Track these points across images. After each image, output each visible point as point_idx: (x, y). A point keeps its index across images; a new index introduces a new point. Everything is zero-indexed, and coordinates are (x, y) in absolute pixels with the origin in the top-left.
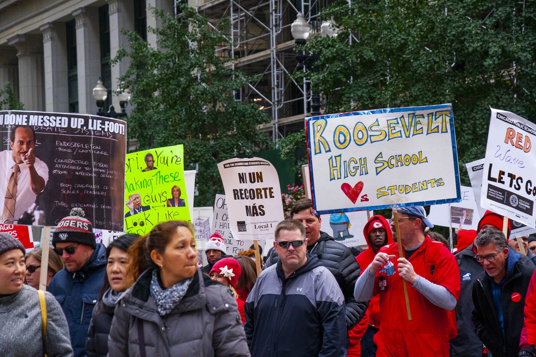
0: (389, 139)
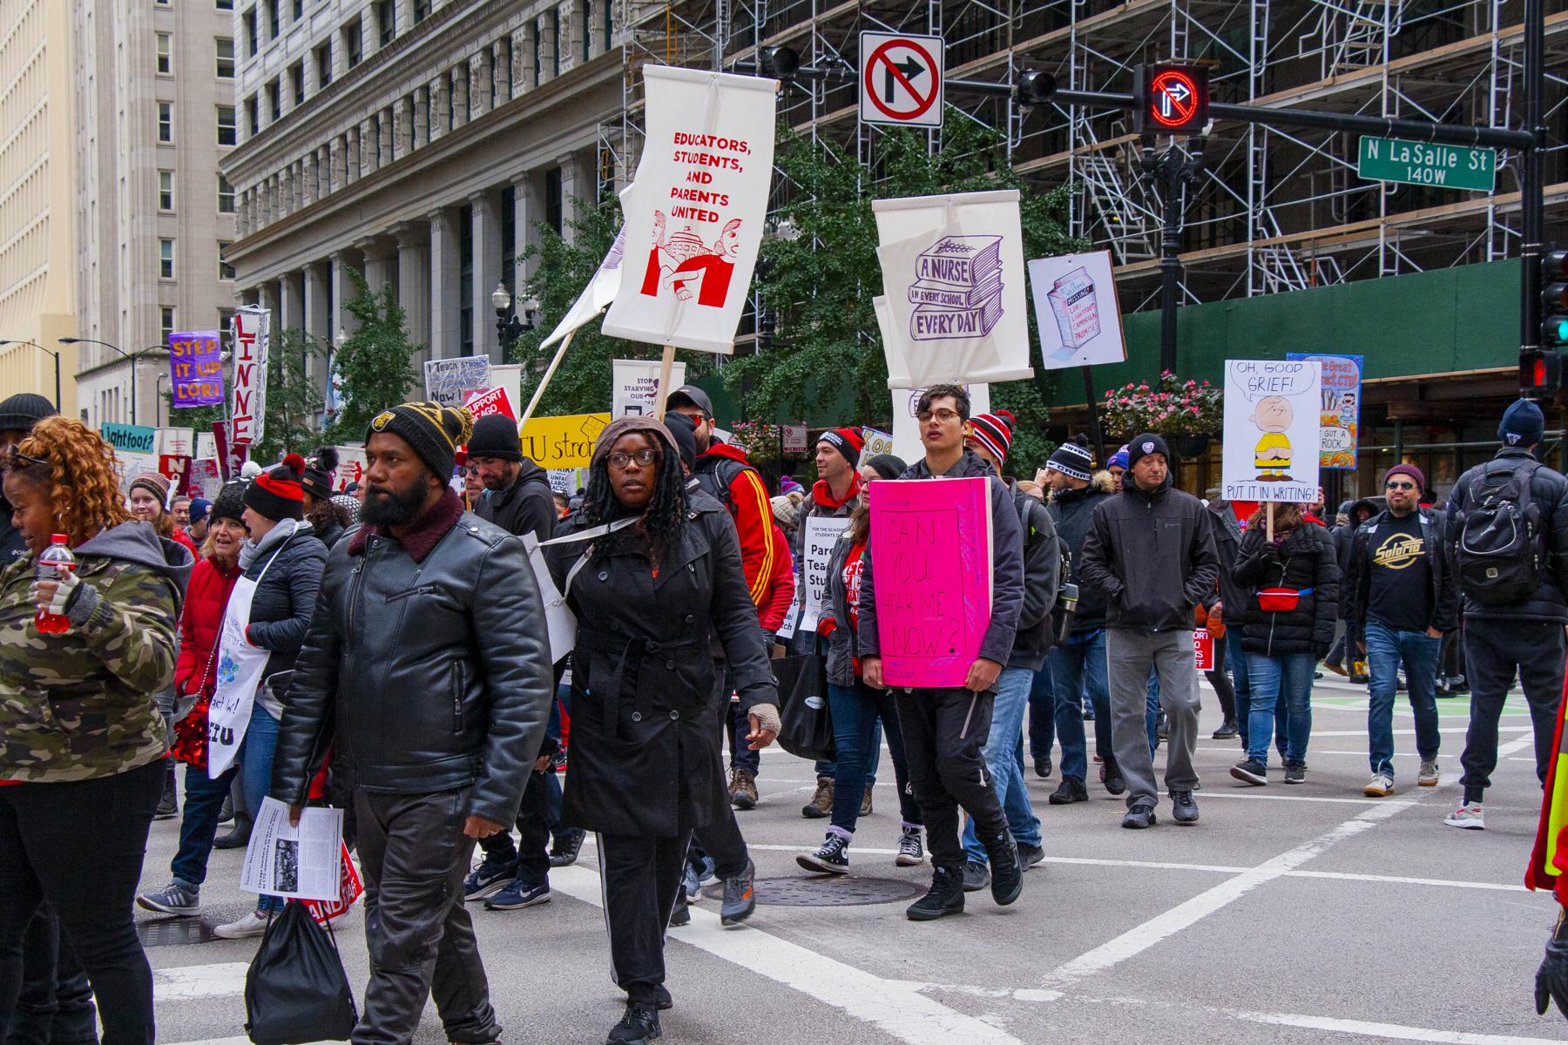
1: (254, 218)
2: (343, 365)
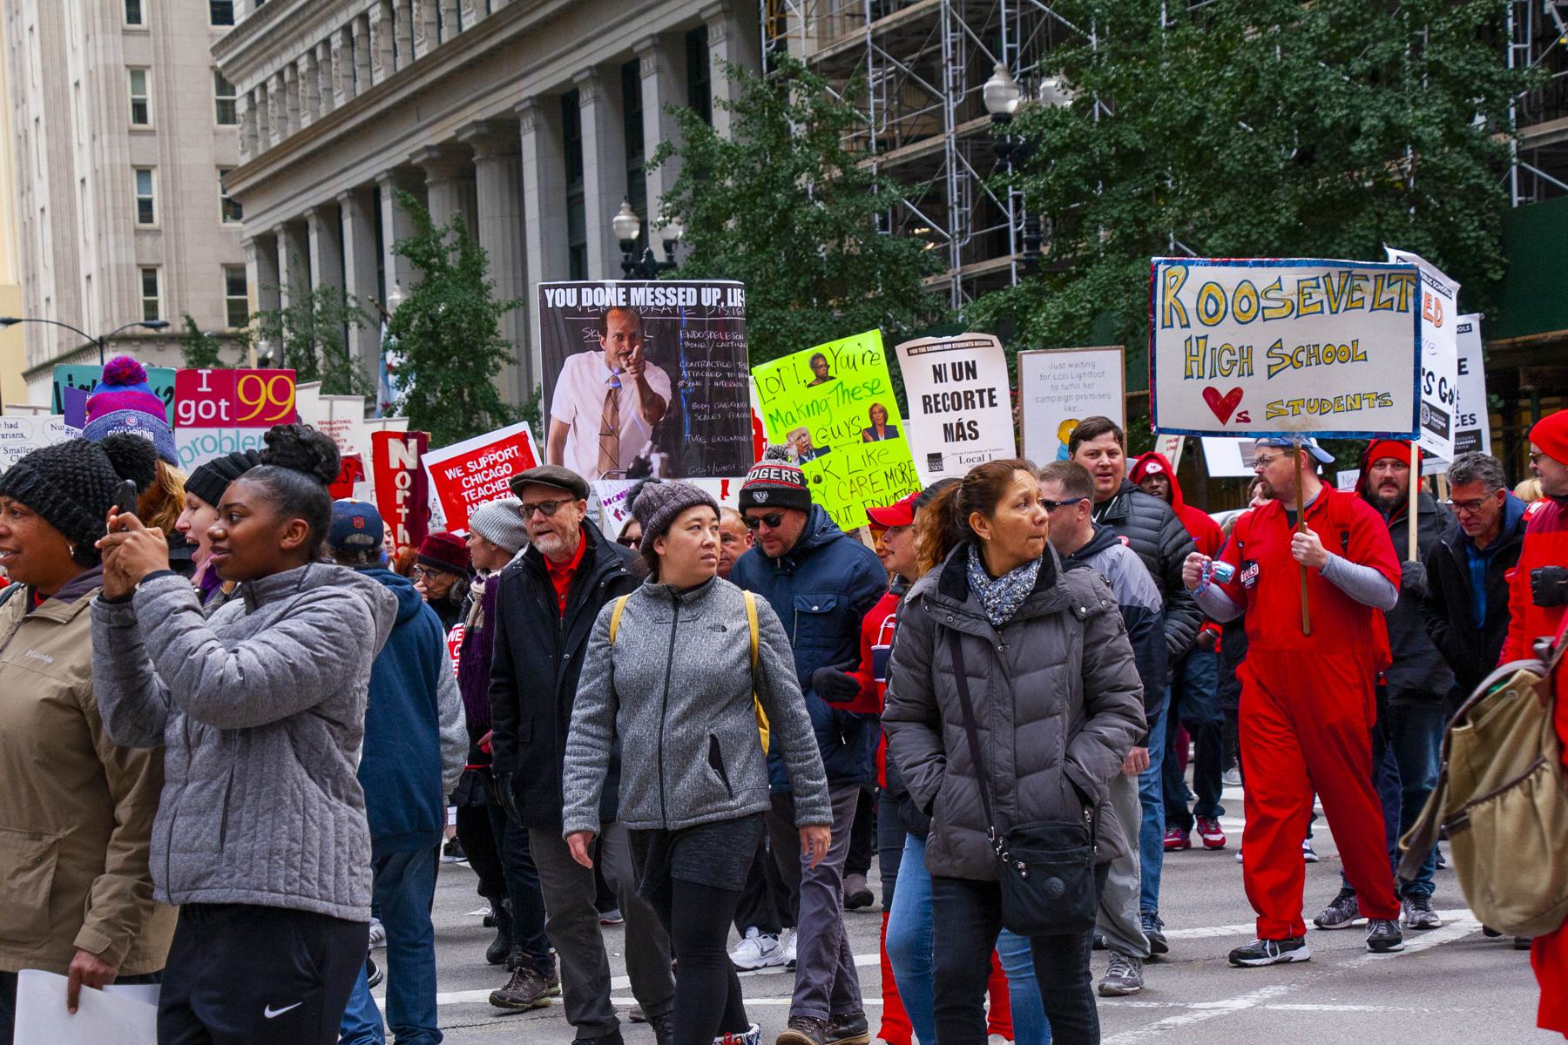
0: (1298, 316)
1: (265, 129)
2: (398, 336)
